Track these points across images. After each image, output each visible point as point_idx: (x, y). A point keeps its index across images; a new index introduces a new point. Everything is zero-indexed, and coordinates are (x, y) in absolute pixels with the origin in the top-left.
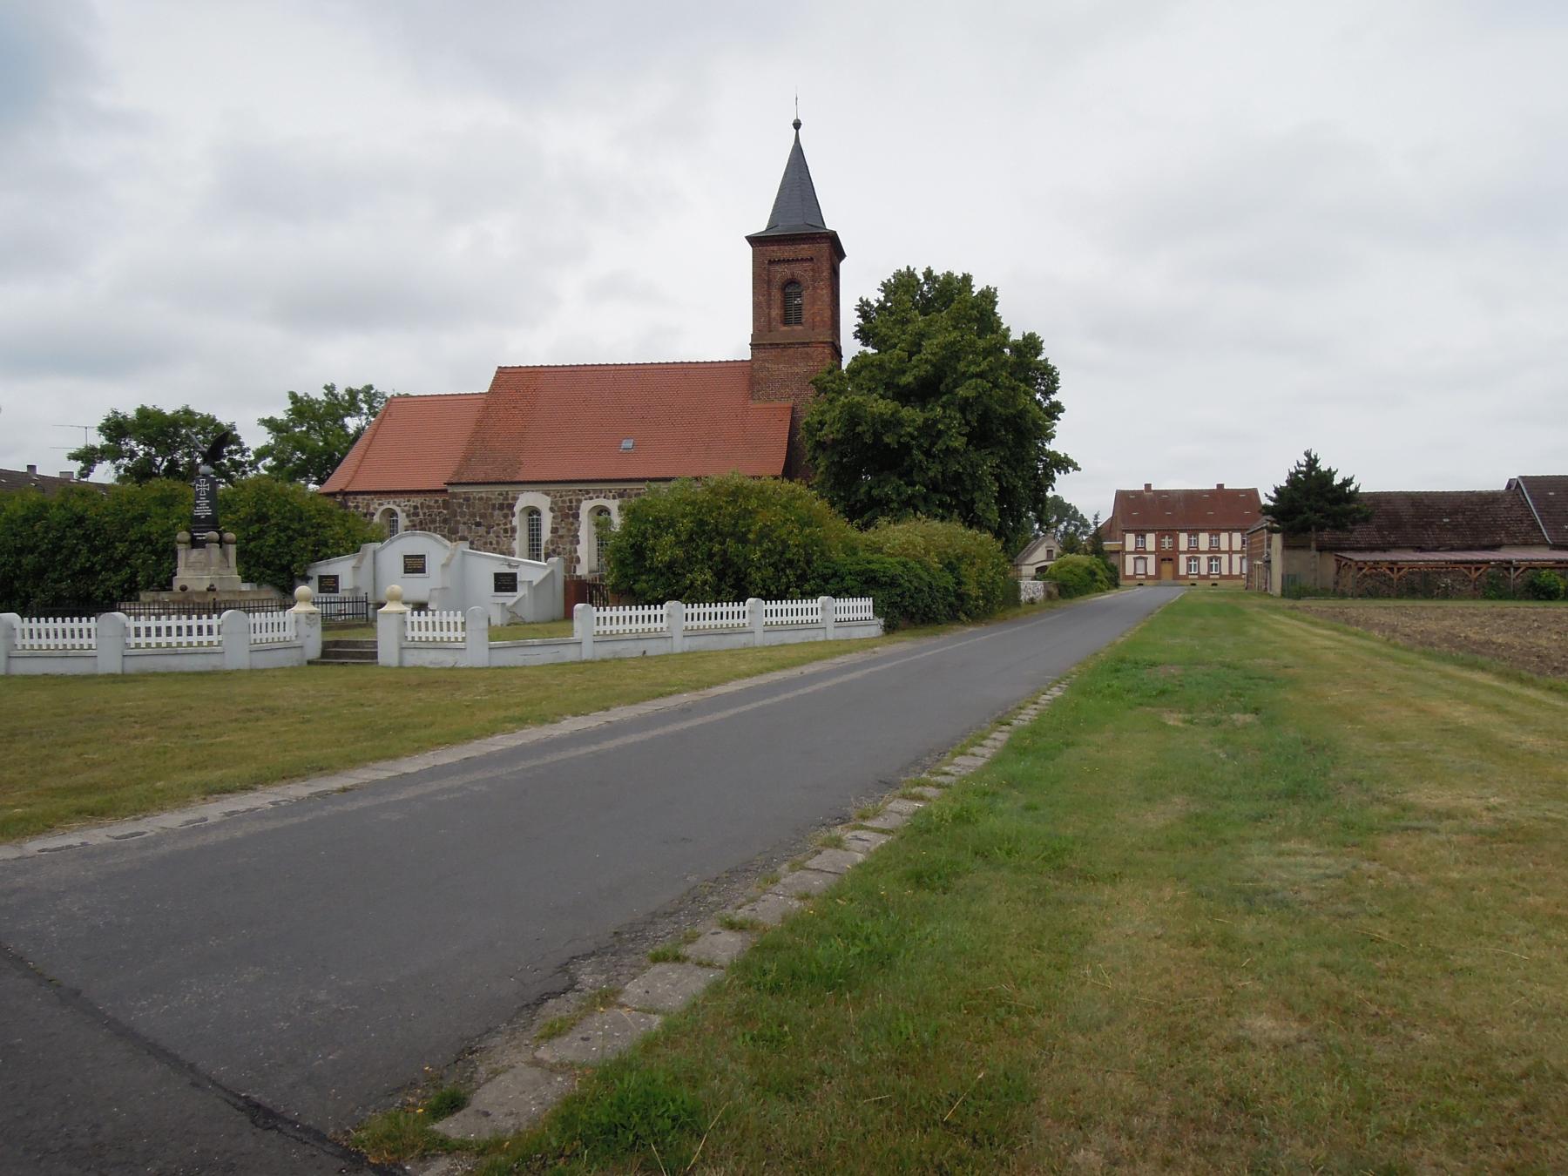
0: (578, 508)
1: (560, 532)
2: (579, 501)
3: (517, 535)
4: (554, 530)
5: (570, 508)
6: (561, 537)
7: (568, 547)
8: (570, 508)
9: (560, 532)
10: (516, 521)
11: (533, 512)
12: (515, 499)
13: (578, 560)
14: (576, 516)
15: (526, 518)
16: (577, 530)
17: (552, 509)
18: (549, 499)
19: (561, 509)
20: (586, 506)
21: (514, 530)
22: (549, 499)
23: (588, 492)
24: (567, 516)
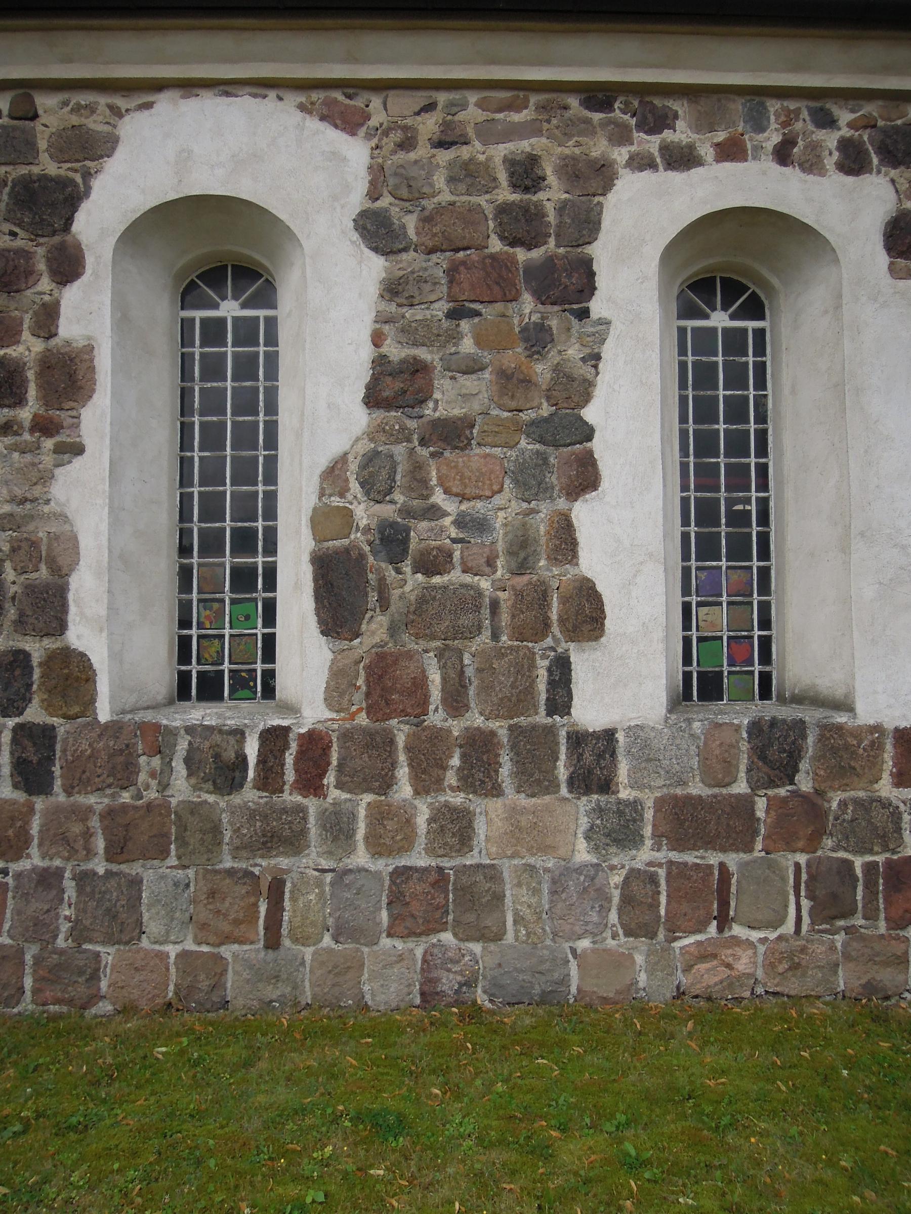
0: (586, 225)
1: (447, 399)
2: (594, 178)
3: (96, 419)
4: (394, 387)
5: (522, 226)
6: (451, 434)
7: (504, 510)
8: (522, 226)
9: (447, 399)
10: (87, 312)
11: (221, 260)
12: (89, 149)
13: (587, 614)
14: (570, 287)
15: (159, 310)
16: (575, 389)
17: (375, 230)
18: (356, 153)
19: (448, 236)
20: (644, 217)
21: (68, 377)
22: (356, 153)
23: (650, 106)
24: (499, 282)
